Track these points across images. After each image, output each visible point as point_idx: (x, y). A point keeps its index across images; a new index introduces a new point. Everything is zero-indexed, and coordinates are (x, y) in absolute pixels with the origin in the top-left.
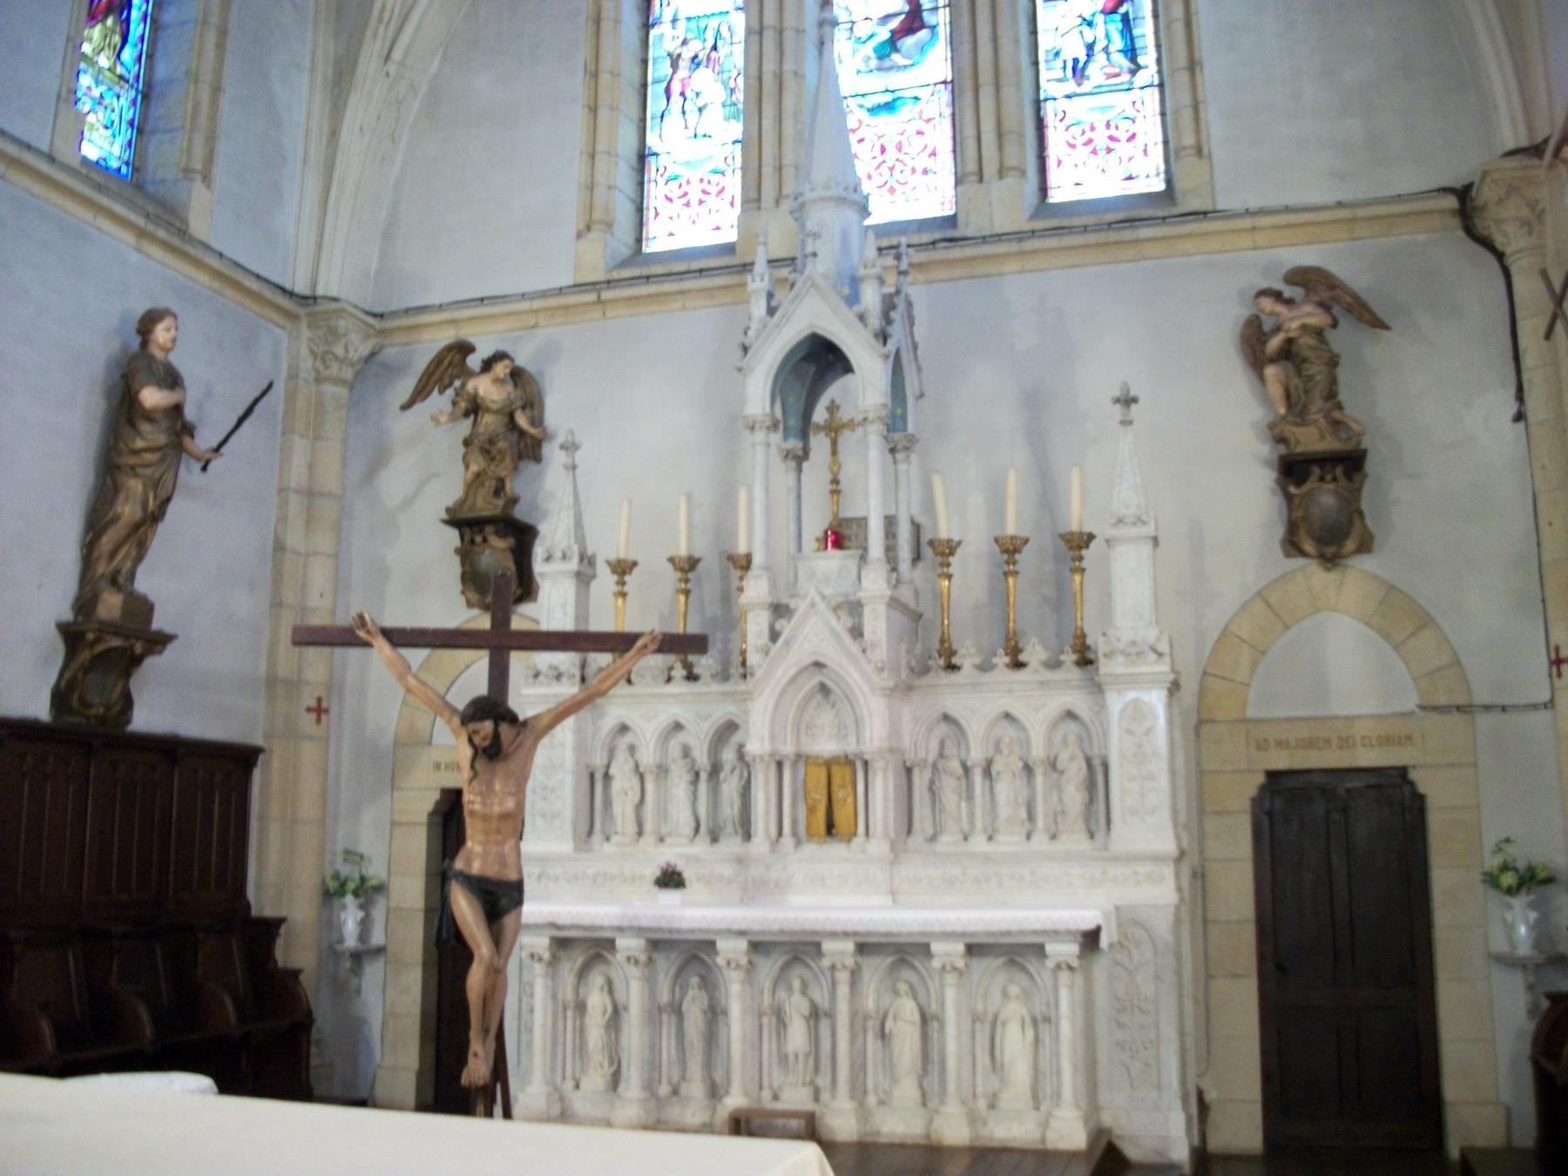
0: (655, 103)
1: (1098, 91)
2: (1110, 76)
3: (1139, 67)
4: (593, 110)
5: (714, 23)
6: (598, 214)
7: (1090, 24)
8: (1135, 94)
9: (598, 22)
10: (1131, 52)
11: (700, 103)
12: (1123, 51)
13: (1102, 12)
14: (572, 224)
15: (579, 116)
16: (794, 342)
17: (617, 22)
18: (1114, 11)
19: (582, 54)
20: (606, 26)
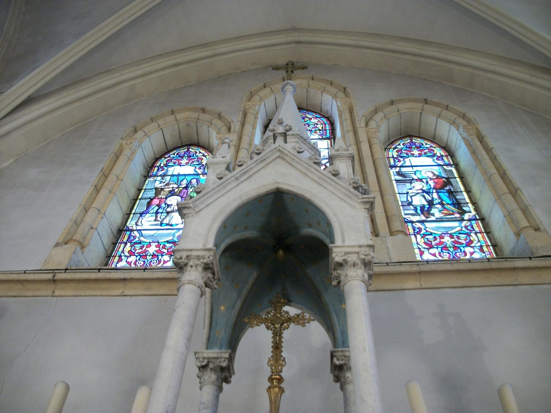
0: (140, 206)
1: (438, 220)
2: (446, 214)
3: (465, 212)
4: (97, 189)
5: (189, 178)
6: (77, 237)
7: (428, 193)
8: (464, 223)
9: (117, 157)
10: (458, 205)
11: (169, 209)
12: (453, 204)
13: (434, 188)
14: (58, 235)
15: (88, 189)
16: (263, 190)
17: (130, 159)
18: (442, 188)
19: (105, 163)
20: (122, 159)
